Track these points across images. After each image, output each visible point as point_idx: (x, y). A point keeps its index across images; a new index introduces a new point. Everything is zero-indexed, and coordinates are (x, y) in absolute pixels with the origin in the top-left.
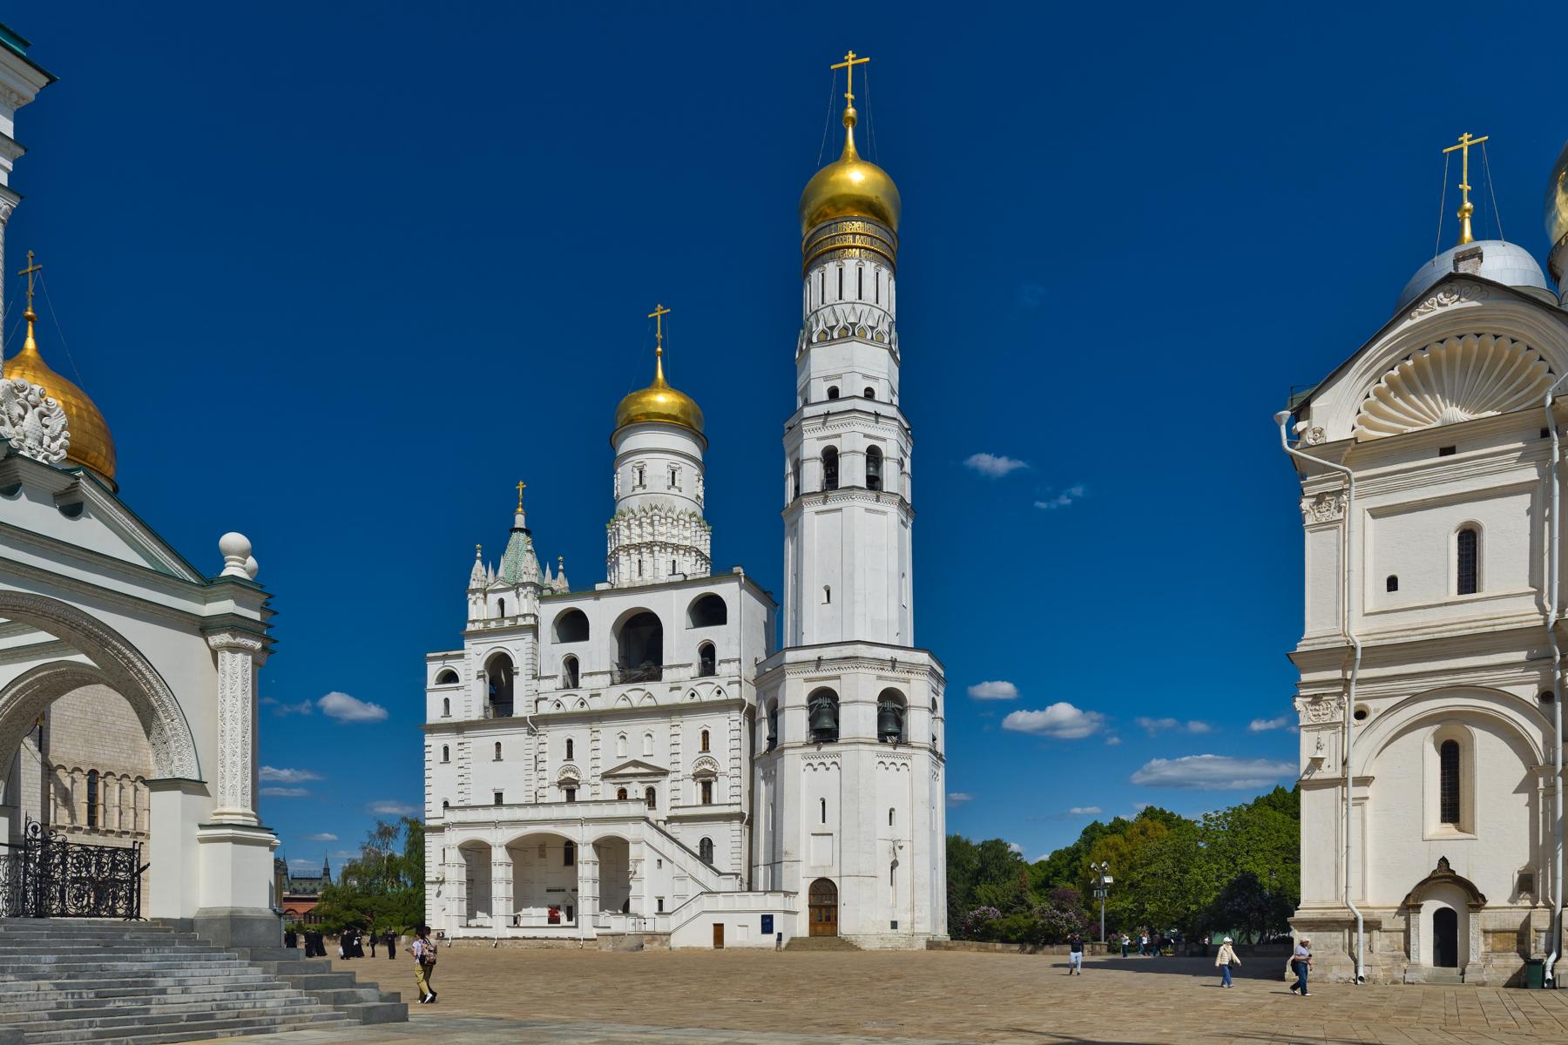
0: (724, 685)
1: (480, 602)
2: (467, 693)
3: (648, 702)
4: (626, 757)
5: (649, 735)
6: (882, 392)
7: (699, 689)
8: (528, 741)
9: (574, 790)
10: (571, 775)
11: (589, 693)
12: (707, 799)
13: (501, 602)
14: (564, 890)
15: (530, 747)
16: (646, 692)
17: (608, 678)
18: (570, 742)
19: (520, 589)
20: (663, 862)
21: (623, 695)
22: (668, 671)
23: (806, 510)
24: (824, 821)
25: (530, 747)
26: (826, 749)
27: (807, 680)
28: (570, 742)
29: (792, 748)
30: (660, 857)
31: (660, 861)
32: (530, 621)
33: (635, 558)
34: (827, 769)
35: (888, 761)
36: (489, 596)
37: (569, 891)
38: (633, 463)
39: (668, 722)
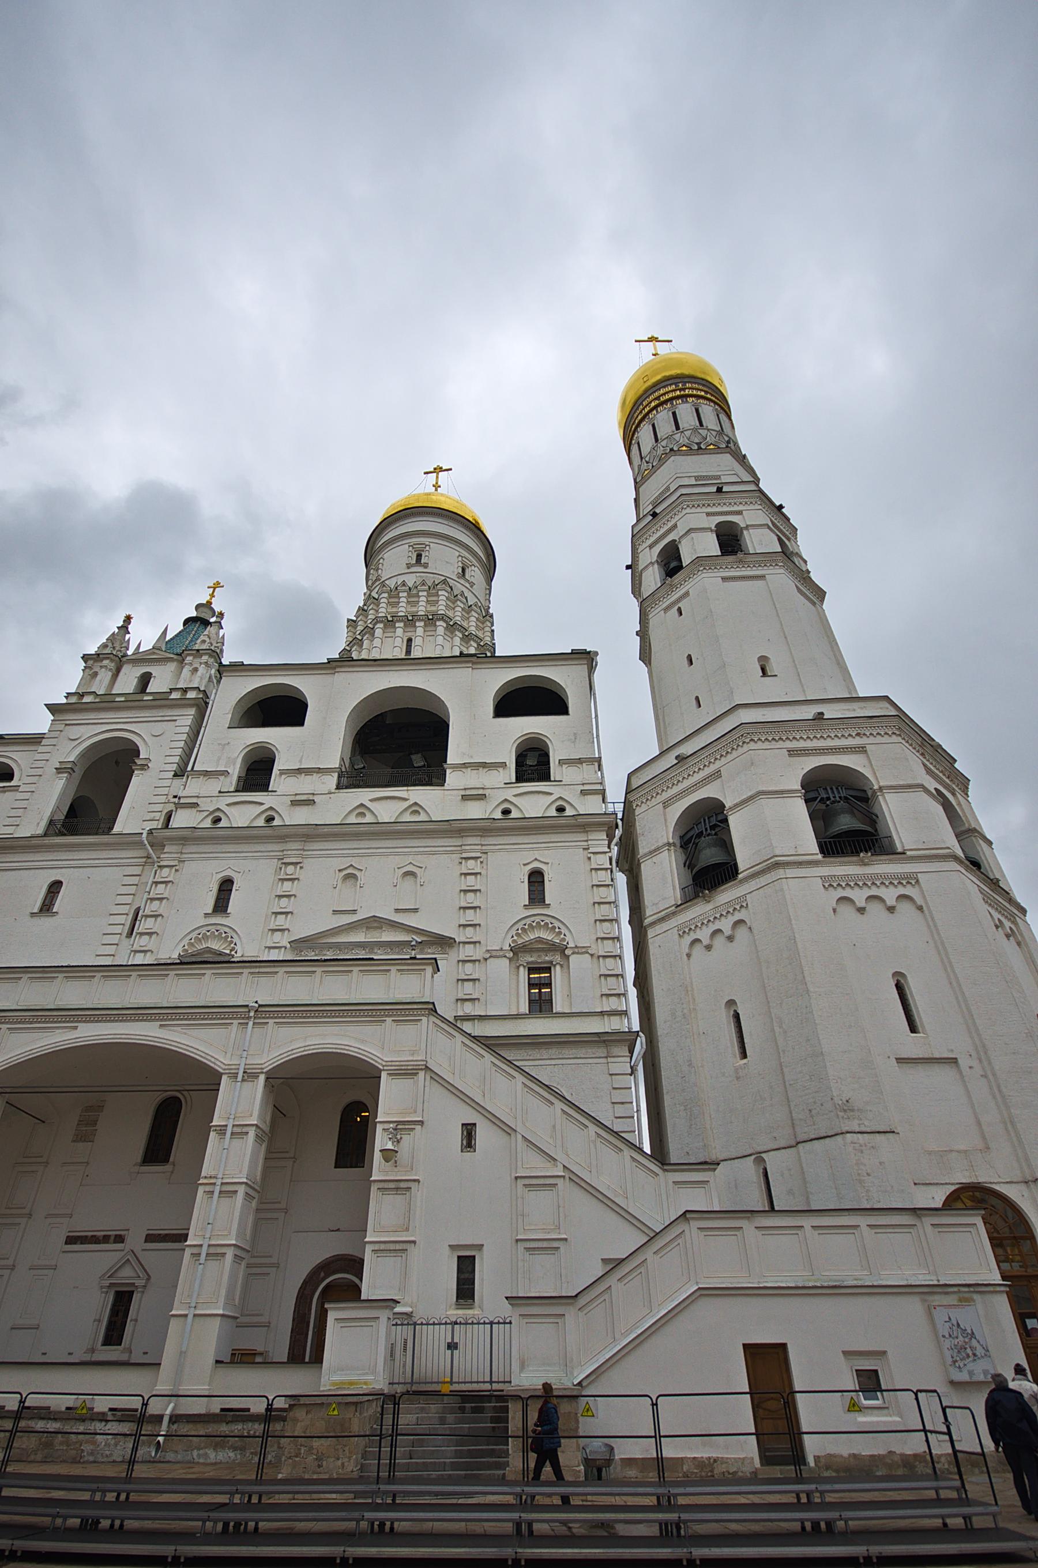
0: (571, 795)
1: (104, 676)
2: (26, 796)
4: (354, 911)
5: (407, 874)
10: (215, 945)
13: (145, 679)
14: (120, 1239)
17: (332, 780)
18: (226, 886)
19: (189, 659)
20: (478, 1129)
21: (362, 805)
22: (458, 774)
23: (704, 575)
27: (792, 753)
28: (226, 886)
29: (800, 864)
30: (471, 1117)
31: (469, 1132)
32: (191, 695)
33: (399, 632)
36: (126, 669)
37: (135, 1241)
39: (452, 852)
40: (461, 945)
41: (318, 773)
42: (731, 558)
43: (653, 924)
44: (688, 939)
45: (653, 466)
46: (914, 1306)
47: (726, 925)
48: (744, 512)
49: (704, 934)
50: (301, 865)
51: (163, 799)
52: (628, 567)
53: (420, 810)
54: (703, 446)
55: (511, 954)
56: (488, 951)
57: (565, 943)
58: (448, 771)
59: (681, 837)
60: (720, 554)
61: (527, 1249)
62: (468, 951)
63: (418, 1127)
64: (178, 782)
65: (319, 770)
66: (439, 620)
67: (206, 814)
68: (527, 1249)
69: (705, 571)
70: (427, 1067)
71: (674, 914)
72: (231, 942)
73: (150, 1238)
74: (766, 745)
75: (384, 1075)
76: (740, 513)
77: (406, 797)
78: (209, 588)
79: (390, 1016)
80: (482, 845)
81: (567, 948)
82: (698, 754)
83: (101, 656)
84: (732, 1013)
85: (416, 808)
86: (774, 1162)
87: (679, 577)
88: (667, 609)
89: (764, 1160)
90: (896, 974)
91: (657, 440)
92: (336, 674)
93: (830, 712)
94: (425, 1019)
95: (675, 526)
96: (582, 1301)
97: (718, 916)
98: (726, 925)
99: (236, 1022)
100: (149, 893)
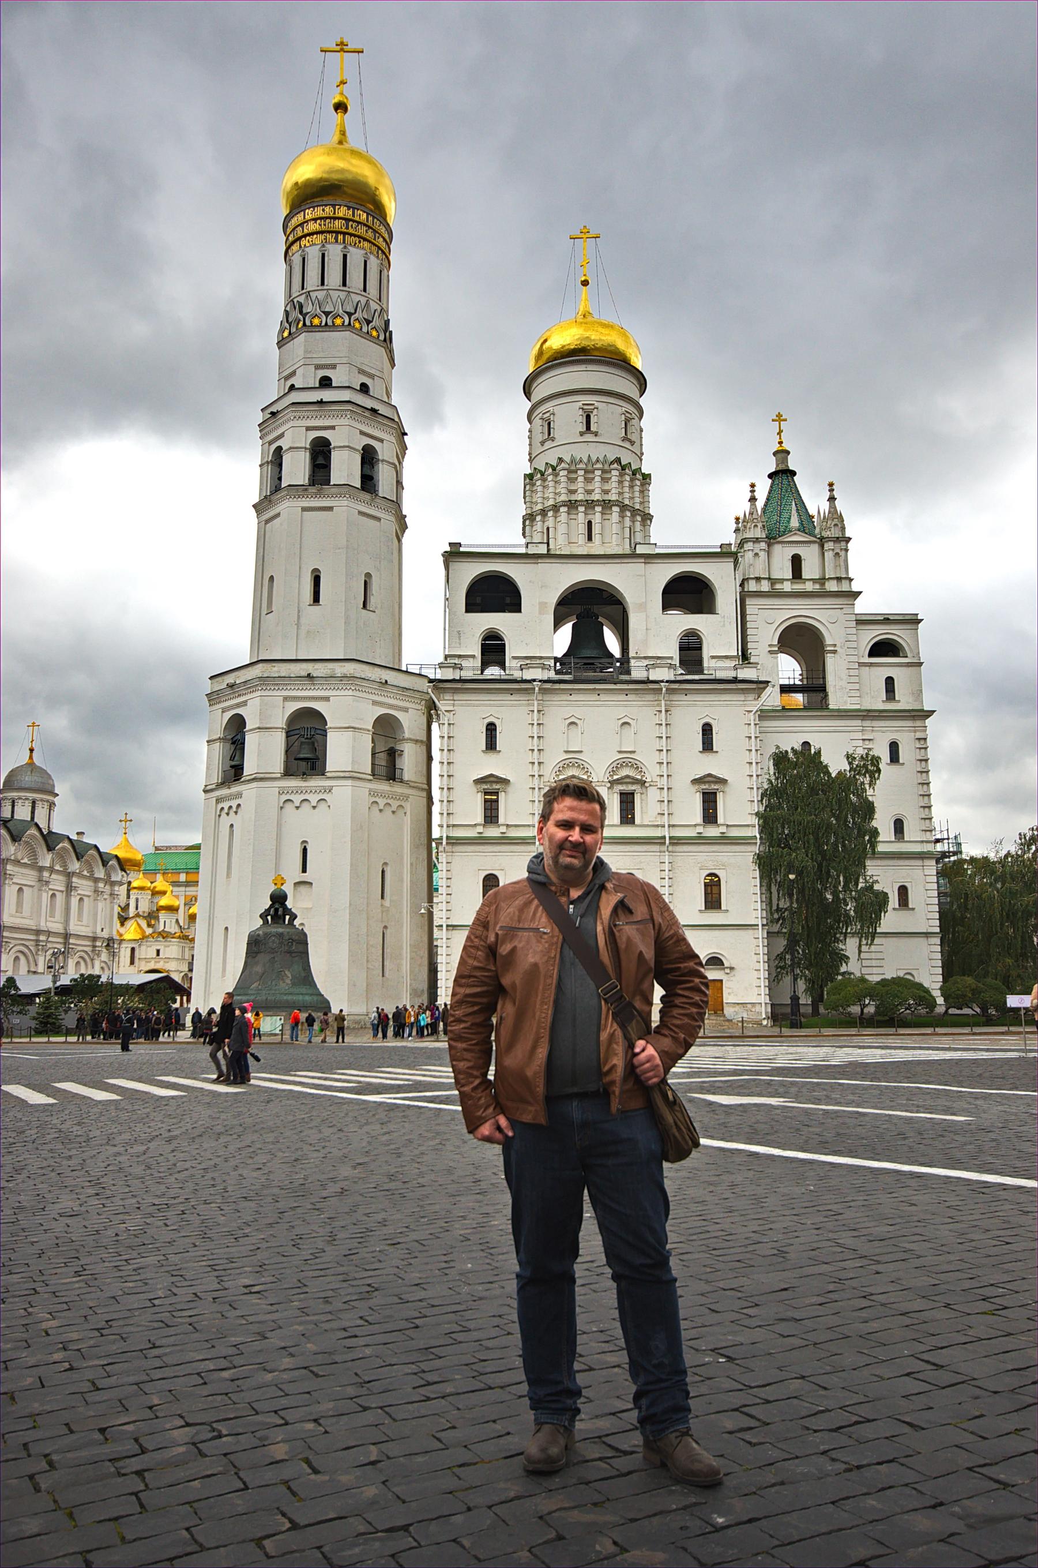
6: (376, 388)
24: (304, 870)
26: (315, 782)
27: (286, 699)
34: (314, 807)
42: (312, 490)
47: (234, 804)
54: (330, 323)
76: (333, 428)
95: (282, 436)
98: (234, 804)
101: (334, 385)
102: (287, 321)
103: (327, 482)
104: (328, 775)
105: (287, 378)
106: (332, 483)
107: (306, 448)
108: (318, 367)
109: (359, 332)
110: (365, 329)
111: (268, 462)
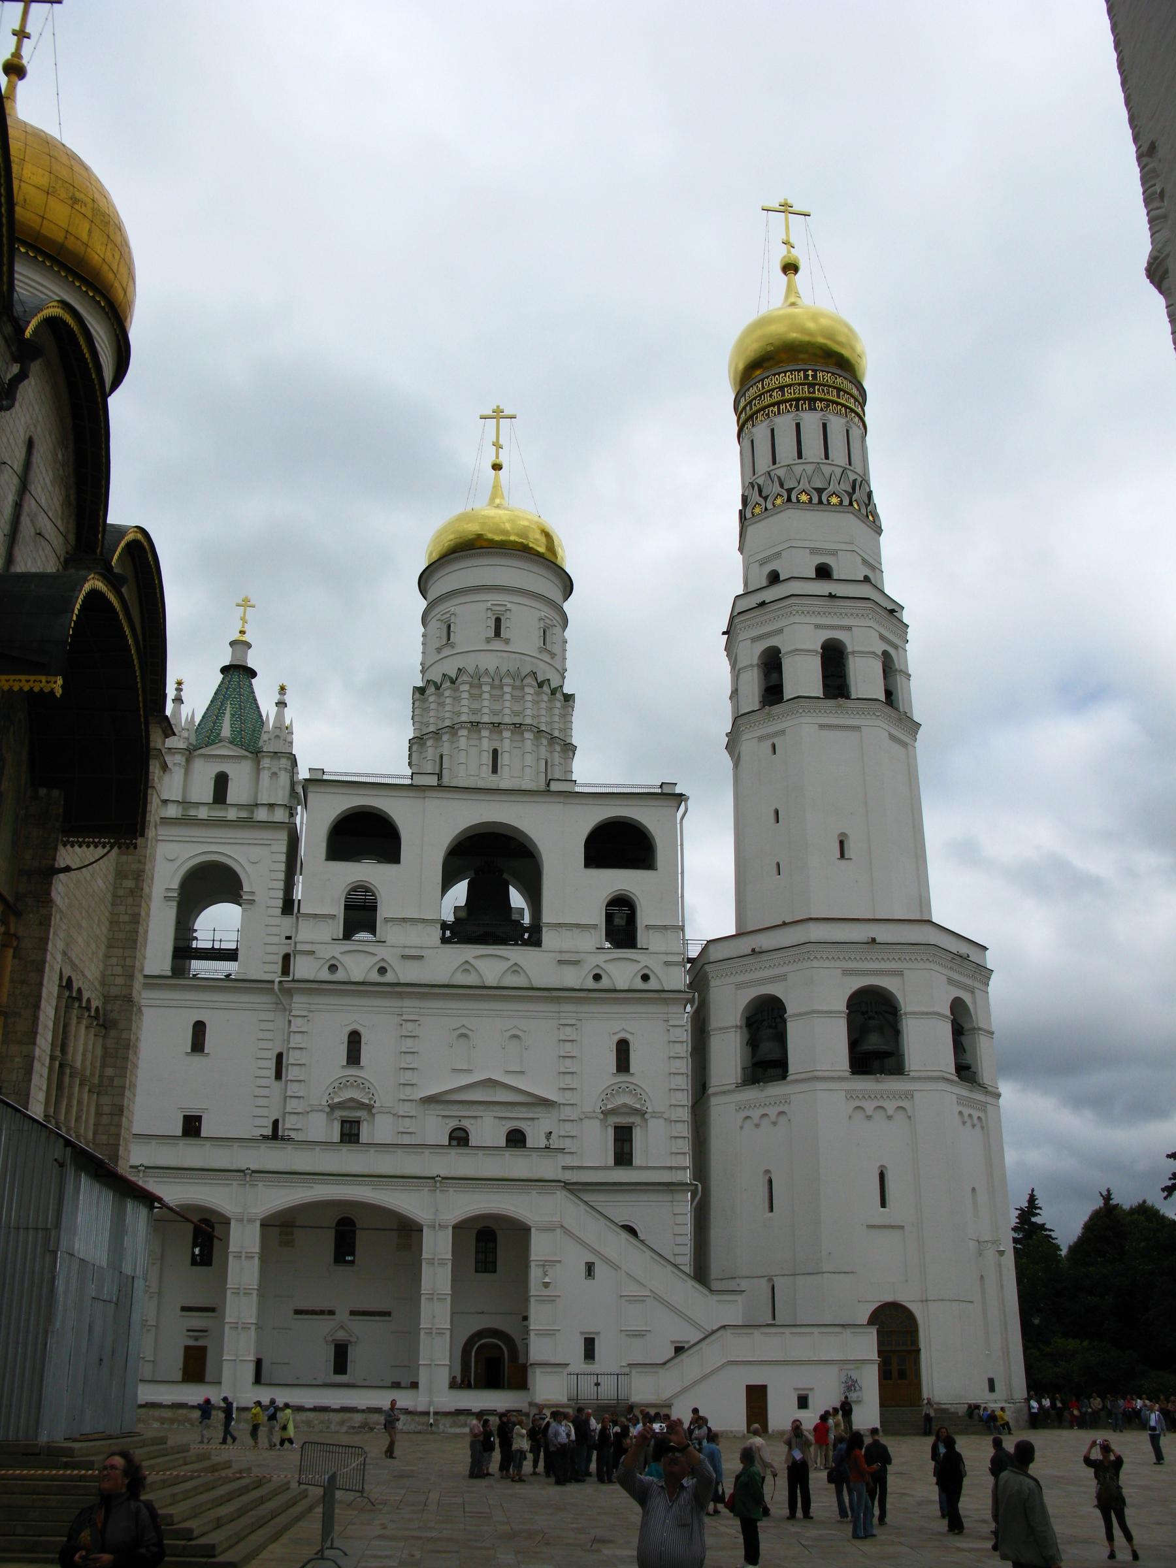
3: (511, 980)
5: (515, 1036)
7: (609, 967)
8: (264, 1025)
9: (357, 1123)
11: (400, 952)
12: (623, 1157)
13: (221, 782)
14: (332, 1313)
15: (269, 1035)
16: (513, 963)
21: (467, 962)
23: (803, 720)
25: (269, 1035)
26: (892, 1084)
27: (847, 972)
28: (355, 1039)
31: (590, 1269)
33: (485, 742)
35: (966, 1111)
37: (342, 1315)
38: (489, 604)
40: (561, 1106)
41: (422, 922)
43: (716, 1094)
44: (742, 1115)
45: (766, 509)
46: (834, 1370)
47: (773, 1112)
48: (853, 628)
49: (756, 1114)
50: (418, 1023)
51: (276, 940)
52: (724, 633)
53: (521, 971)
55: (602, 1116)
56: (584, 1112)
57: (645, 1109)
58: (544, 930)
59: (748, 1019)
60: (819, 692)
61: (627, 1335)
62: (567, 1112)
63: (558, 1265)
64: (288, 921)
65: (424, 921)
66: (527, 730)
67: (324, 961)
68: (627, 1335)
69: (803, 714)
70: (562, 1226)
71: (733, 1091)
72: (369, 1092)
73: (353, 1313)
74: (827, 964)
75: (533, 1230)
76: (849, 628)
77: (508, 957)
78: (238, 605)
79: (535, 1189)
80: (577, 1013)
81: (646, 1112)
82: (771, 953)
83: (173, 751)
84: (767, 1178)
85: (516, 968)
86: (778, 1282)
87: (777, 709)
88: (761, 739)
89: (773, 1280)
90: (882, 1166)
91: (774, 463)
92: (427, 799)
93: (883, 934)
94: (558, 1192)
95: (780, 631)
96: (668, 1365)
97: (768, 1103)
98: (773, 1112)
99: (426, 1189)
100: (289, 1042)
101: (835, 577)
102: (760, 495)
103: (847, 697)
104: (912, 1074)
105: (762, 563)
106: (853, 697)
107: (816, 651)
108: (814, 551)
109: (857, 514)
110: (864, 511)
111: (752, 666)
